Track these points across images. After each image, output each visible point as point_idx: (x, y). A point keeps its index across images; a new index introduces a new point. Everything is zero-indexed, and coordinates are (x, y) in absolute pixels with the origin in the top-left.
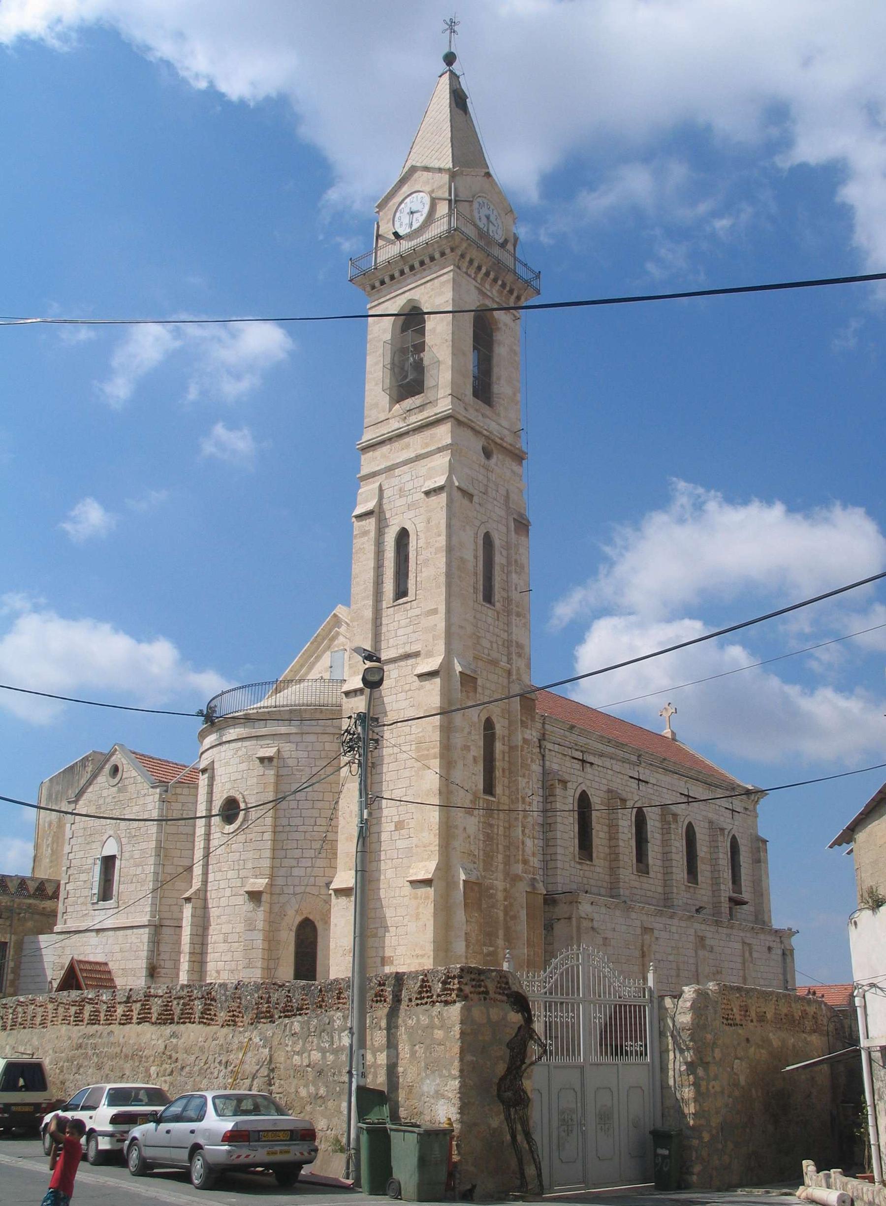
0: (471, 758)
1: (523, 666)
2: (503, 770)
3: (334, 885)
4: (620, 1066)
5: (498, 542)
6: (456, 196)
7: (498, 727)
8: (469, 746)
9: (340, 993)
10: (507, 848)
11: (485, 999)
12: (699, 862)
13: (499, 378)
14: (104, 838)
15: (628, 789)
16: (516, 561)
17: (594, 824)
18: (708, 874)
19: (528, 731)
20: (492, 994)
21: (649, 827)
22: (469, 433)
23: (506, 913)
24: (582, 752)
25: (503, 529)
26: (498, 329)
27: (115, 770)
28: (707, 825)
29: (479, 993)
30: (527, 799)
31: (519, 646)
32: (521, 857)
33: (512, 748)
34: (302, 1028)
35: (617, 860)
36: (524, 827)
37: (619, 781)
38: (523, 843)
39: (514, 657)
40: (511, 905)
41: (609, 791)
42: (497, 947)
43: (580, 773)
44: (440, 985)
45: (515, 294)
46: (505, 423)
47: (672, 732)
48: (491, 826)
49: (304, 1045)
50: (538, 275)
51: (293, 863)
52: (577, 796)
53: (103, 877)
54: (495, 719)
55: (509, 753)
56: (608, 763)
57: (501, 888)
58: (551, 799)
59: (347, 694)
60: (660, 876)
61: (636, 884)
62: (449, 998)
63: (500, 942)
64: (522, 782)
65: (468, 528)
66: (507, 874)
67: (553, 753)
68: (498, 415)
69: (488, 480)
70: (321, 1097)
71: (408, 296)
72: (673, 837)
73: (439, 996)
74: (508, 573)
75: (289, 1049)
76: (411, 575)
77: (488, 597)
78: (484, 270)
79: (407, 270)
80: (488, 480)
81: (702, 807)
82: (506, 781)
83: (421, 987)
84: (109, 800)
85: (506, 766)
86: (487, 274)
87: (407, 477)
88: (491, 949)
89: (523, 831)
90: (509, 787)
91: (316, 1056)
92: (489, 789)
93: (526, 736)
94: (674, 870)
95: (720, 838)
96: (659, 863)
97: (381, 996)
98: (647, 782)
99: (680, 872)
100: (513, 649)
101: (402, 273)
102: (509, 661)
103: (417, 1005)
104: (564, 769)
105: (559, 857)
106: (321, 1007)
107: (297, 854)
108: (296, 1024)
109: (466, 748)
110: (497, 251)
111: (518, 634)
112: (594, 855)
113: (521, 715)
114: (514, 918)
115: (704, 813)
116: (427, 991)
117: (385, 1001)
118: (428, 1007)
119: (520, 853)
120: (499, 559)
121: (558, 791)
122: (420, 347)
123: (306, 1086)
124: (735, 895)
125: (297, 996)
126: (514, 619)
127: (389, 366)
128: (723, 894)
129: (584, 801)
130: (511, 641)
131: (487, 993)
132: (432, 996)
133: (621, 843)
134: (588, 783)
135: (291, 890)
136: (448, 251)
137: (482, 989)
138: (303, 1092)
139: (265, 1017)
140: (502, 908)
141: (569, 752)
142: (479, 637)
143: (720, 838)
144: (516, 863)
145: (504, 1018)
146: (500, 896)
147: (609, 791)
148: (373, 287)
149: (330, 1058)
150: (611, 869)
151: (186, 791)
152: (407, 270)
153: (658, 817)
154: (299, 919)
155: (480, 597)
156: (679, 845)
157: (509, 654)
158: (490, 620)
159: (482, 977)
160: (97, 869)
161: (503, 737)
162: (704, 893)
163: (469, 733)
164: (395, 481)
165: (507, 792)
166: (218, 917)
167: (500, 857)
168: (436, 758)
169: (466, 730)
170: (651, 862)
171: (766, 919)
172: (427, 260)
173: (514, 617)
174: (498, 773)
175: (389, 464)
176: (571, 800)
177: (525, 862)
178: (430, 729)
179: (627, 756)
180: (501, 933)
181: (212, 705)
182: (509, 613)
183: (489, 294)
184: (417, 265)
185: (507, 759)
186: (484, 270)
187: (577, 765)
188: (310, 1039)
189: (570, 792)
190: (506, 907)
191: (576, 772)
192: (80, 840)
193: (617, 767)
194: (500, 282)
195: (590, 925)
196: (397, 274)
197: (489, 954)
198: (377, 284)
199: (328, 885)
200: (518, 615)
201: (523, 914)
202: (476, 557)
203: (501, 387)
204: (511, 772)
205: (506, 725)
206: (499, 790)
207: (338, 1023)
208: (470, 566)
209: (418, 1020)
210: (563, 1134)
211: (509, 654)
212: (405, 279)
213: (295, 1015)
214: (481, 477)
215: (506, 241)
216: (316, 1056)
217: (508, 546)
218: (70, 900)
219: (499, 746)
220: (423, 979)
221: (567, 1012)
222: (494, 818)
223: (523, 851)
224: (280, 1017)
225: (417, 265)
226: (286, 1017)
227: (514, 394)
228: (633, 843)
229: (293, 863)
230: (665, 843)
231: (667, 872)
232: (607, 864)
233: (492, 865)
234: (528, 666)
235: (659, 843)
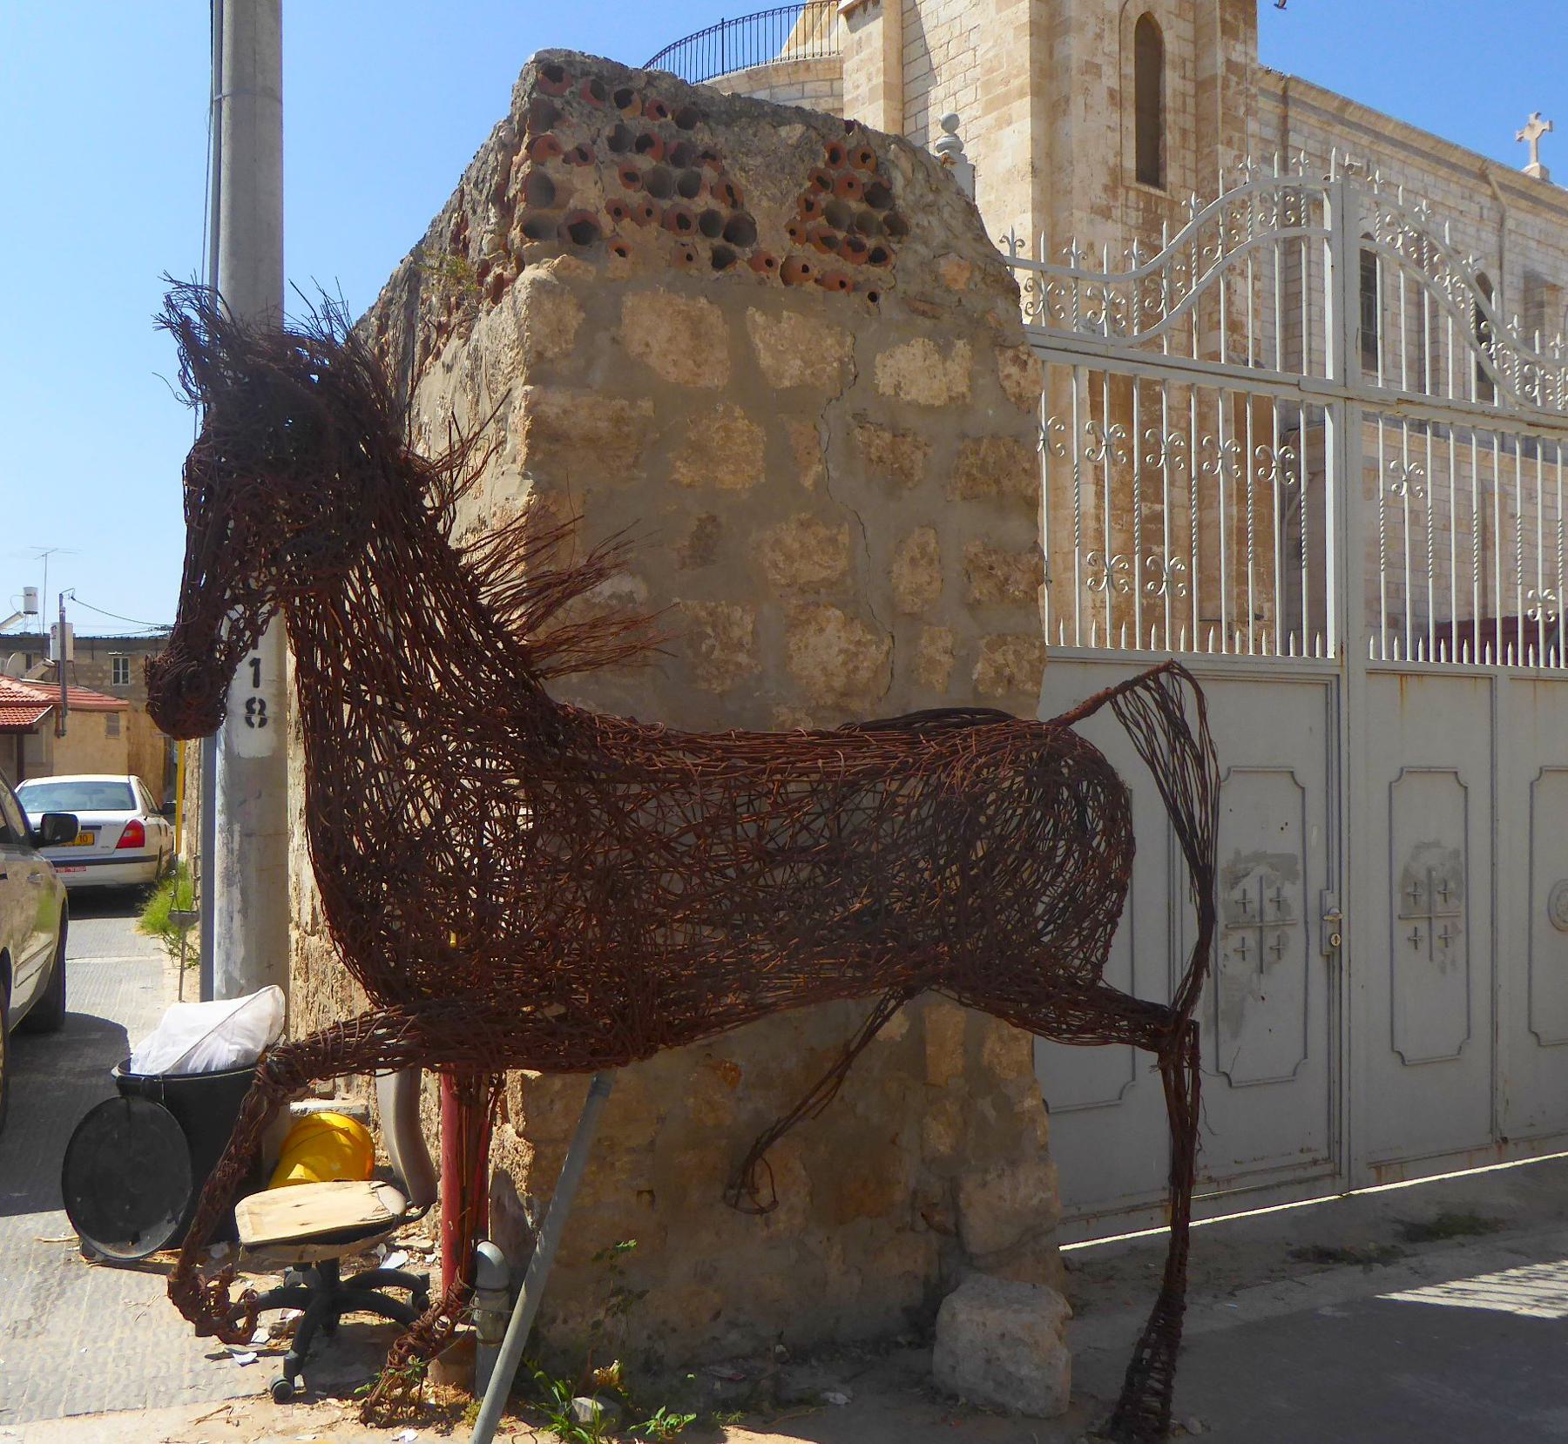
0: (1105, 95)
2: (1184, 132)
4: (1503, 685)
7: (1168, 37)
8: (1098, 67)
19: (1239, 47)
33: (1203, 86)
47: (1542, 168)
54: (1161, 18)
55: (1196, 95)
82: (1190, 157)
85: (1190, 124)
90: (1197, 171)
92: (1151, 170)
93: (1235, 57)
109: (1093, 69)
163: (1099, 37)
165: (1192, 181)
168: (1021, 95)
169: (1092, 29)
174: (1171, 138)
178: (1010, 33)
185: (1191, 108)
204: (1201, 137)
205: (1189, 34)
206: (1172, 174)
219: (1172, 81)
221: (1264, 486)
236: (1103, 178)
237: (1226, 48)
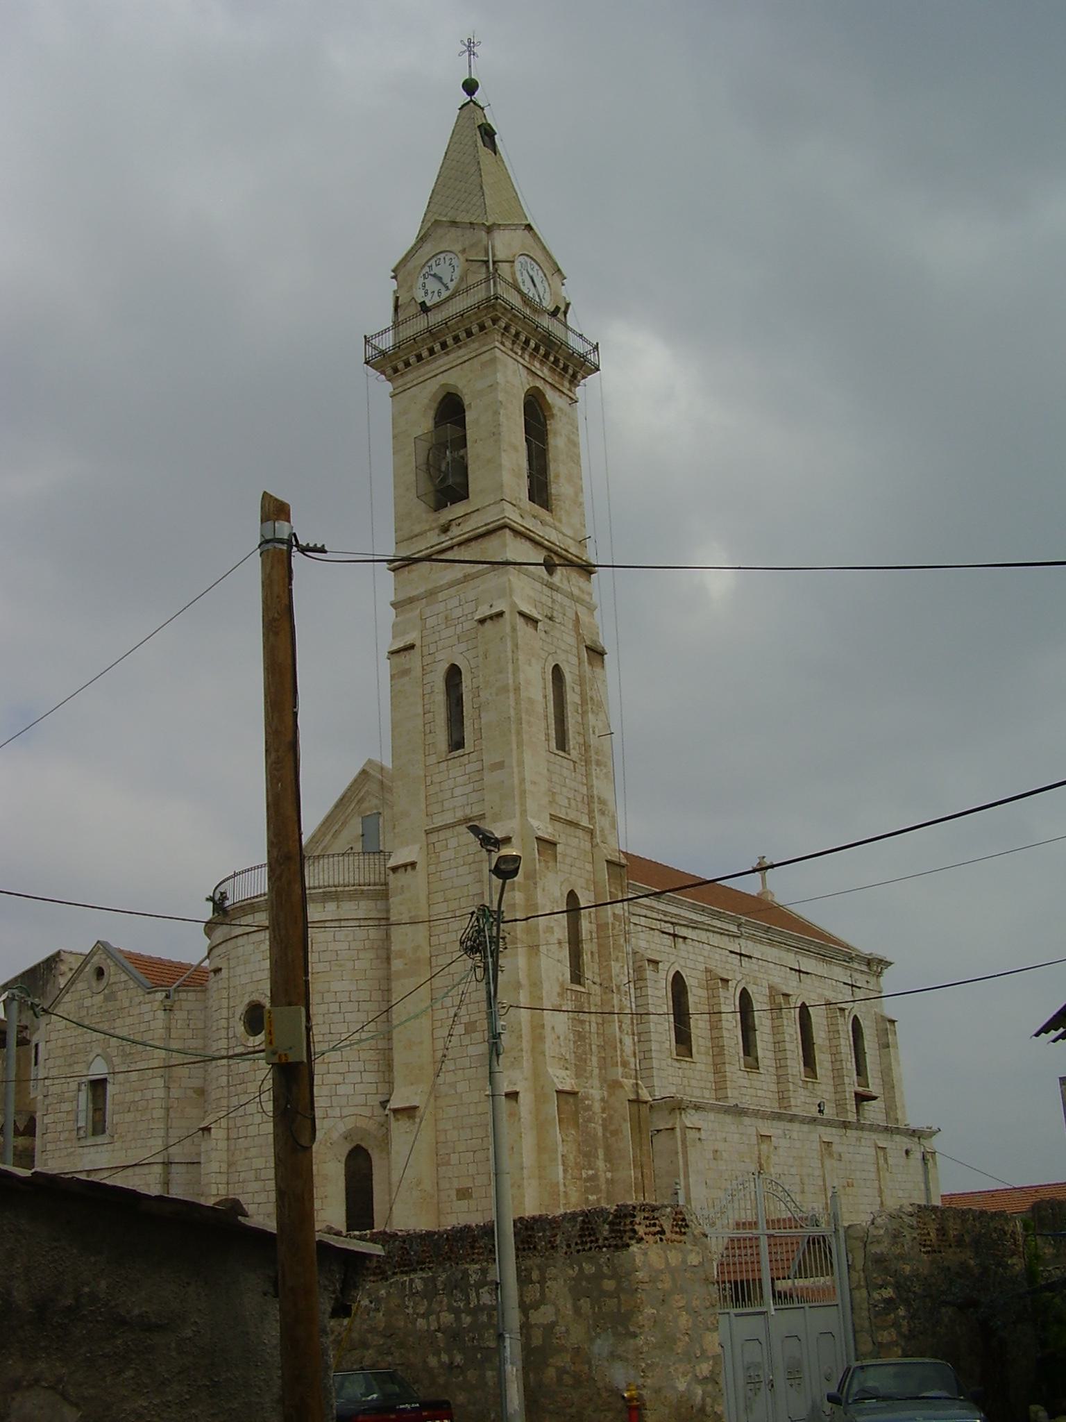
1: (607, 826)
3: (394, 1104)
5: (568, 678)
6: (494, 256)
9: (474, 1241)
10: (602, 1048)
11: (661, 1240)
12: (816, 1052)
13: (557, 476)
14: (91, 1058)
15: (728, 966)
16: (592, 698)
18: (828, 1065)
20: (668, 1235)
22: (528, 544)
23: (605, 1128)
25: (575, 661)
26: (553, 416)
27: (100, 973)
29: (654, 1234)
31: (602, 801)
34: (426, 1285)
35: (721, 1054)
37: (717, 957)
39: (596, 814)
40: (611, 1117)
41: (707, 970)
42: (597, 1170)
44: (607, 1227)
45: (571, 371)
46: (569, 532)
49: (430, 1304)
50: (596, 348)
51: (339, 1079)
52: (670, 979)
53: (91, 1106)
56: (703, 936)
57: (598, 1097)
59: (395, 869)
60: (773, 1070)
61: (746, 1083)
62: (619, 1242)
63: (601, 1164)
64: (615, 967)
65: (533, 661)
66: (603, 1080)
67: (639, 928)
68: (560, 521)
69: (553, 601)
70: (458, 1366)
71: (442, 379)
73: (606, 1239)
74: (584, 714)
75: (410, 1311)
76: (467, 722)
77: (562, 744)
78: (532, 344)
79: (437, 347)
80: (553, 601)
81: (817, 984)
82: (596, 966)
83: (582, 1229)
84: (94, 1011)
85: (595, 949)
86: (537, 349)
87: (454, 602)
88: (590, 1172)
89: (620, 1027)
91: (447, 1318)
94: (789, 1062)
95: (841, 1021)
96: (770, 1055)
97: (528, 1242)
98: (750, 957)
99: (796, 1065)
100: (596, 806)
101: (431, 351)
102: (591, 818)
103: (578, 1251)
104: (653, 946)
105: (654, 1055)
106: (450, 1258)
107: (343, 1067)
108: (418, 1280)
110: (546, 321)
111: (601, 787)
112: (694, 1050)
114: (615, 1133)
115: (819, 990)
116: (590, 1235)
117: (535, 1248)
118: (593, 1253)
120: (572, 697)
121: (649, 973)
122: (462, 442)
123: (437, 1353)
124: (860, 1089)
125: (415, 1247)
126: (594, 769)
127: (424, 467)
129: (678, 985)
130: (592, 797)
131: (662, 1232)
132: (597, 1240)
133: (725, 1034)
135: (337, 1112)
136: (489, 323)
137: (658, 1229)
138: (433, 1361)
139: (375, 1274)
141: (657, 925)
142: (554, 794)
143: (841, 1021)
145: (684, 1261)
146: (597, 1107)
147: (707, 970)
148: (396, 370)
149: (467, 1320)
150: (715, 1065)
151: (191, 996)
152: (437, 347)
153: (766, 999)
154: (347, 1148)
155: (553, 744)
156: (792, 1031)
157: (591, 812)
158: (566, 772)
159: (656, 1214)
160: (84, 1096)
162: (825, 1088)
164: (441, 607)
166: (247, 1149)
167: (594, 1059)
170: (760, 1053)
171: (900, 1116)
172: (463, 335)
173: (594, 767)
174: (586, 958)
175: (430, 586)
177: (625, 1064)
179: (725, 926)
180: (601, 1153)
181: (222, 889)
182: (587, 762)
183: (539, 373)
184: (450, 341)
186: (532, 344)
187: (668, 940)
188: (438, 1298)
189: (662, 974)
190: (604, 1120)
191: (668, 950)
192: (58, 1062)
193: (715, 939)
194: (552, 359)
195: (698, 1136)
196: (425, 353)
197: (590, 1179)
198: (401, 366)
199: (384, 1104)
200: (598, 763)
201: (627, 1127)
202: (545, 697)
203: (559, 488)
204: (603, 956)
207: (473, 1278)
208: (540, 709)
209: (581, 1269)
210: (750, 1394)
211: (591, 812)
212: (435, 360)
213: (415, 1270)
214: (544, 599)
215: (558, 308)
216: (447, 1318)
217: (581, 681)
218: (49, 1136)
220: (583, 1221)
223: (622, 1050)
224: (394, 1274)
225: (450, 341)
226: (402, 1272)
227: (577, 495)
229: (339, 1079)
230: (776, 1030)
231: (781, 1065)
232: (710, 1059)
234: (614, 825)
235: (768, 1030)
236: (557, 989)
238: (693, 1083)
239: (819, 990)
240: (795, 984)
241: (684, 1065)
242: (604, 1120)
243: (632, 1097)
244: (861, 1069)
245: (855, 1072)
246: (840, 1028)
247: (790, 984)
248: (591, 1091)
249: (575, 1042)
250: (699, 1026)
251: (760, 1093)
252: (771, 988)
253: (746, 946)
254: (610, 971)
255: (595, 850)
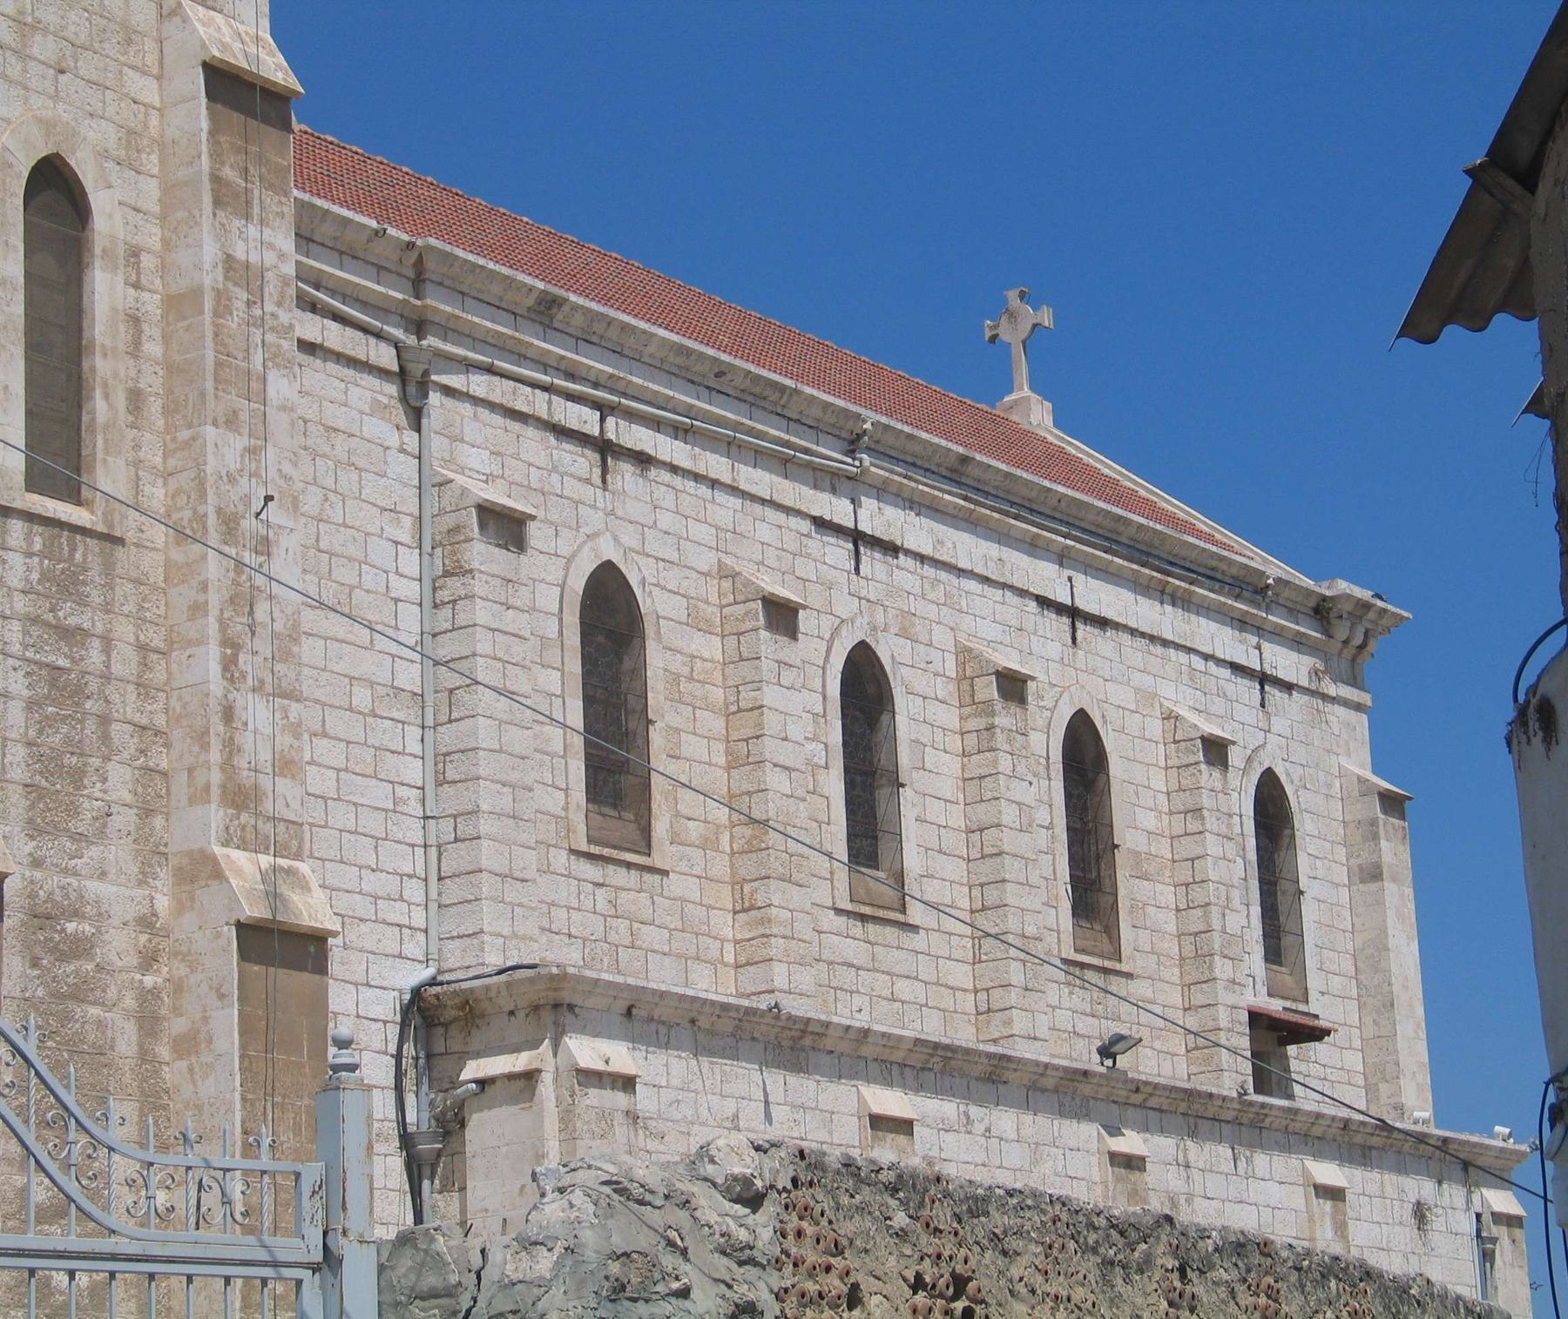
2: (136, 399)
12: (1121, 875)
17: (656, 699)
21: (901, 720)
23: (149, 1023)
24: (597, 405)
28: (1155, 728)
30: (248, 524)
32: (216, 777)
36: (232, 646)
38: (228, 714)
43: (588, 493)
48: (71, 636)
52: (578, 584)
58: (454, 586)
66: (151, 854)
72: (1005, 763)
89: (228, 664)
93: (239, 252)
94: (1012, 894)
113: (216, 156)
119: (215, 756)
124: (1275, 1006)
128: (1226, 998)
133: (777, 781)
134: (630, 538)
140: (130, 1002)
144: (192, 800)
161: (134, 253)
170: (913, 861)
176: (548, 599)
187: (583, 461)
190: (148, 997)
191: (573, 488)
222: (82, 602)
223: (231, 747)
228: (834, 784)
233: (74, 811)
237: (222, 233)
238: (653, 936)
239: (1138, 679)
240: (1055, 649)
241: (619, 876)
242: (148, 997)
243: (254, 910)
244: (1279, 937)
245: (1258, 952)
246: (1206, 801)
247: (1039, 649)
248: (93, 887)
249: (32, 705)
250: (683, 744)
251: (904, 988)
252: (965, 654)
253: (875, 517)
254: (200, 465)
255: (171, 27)
